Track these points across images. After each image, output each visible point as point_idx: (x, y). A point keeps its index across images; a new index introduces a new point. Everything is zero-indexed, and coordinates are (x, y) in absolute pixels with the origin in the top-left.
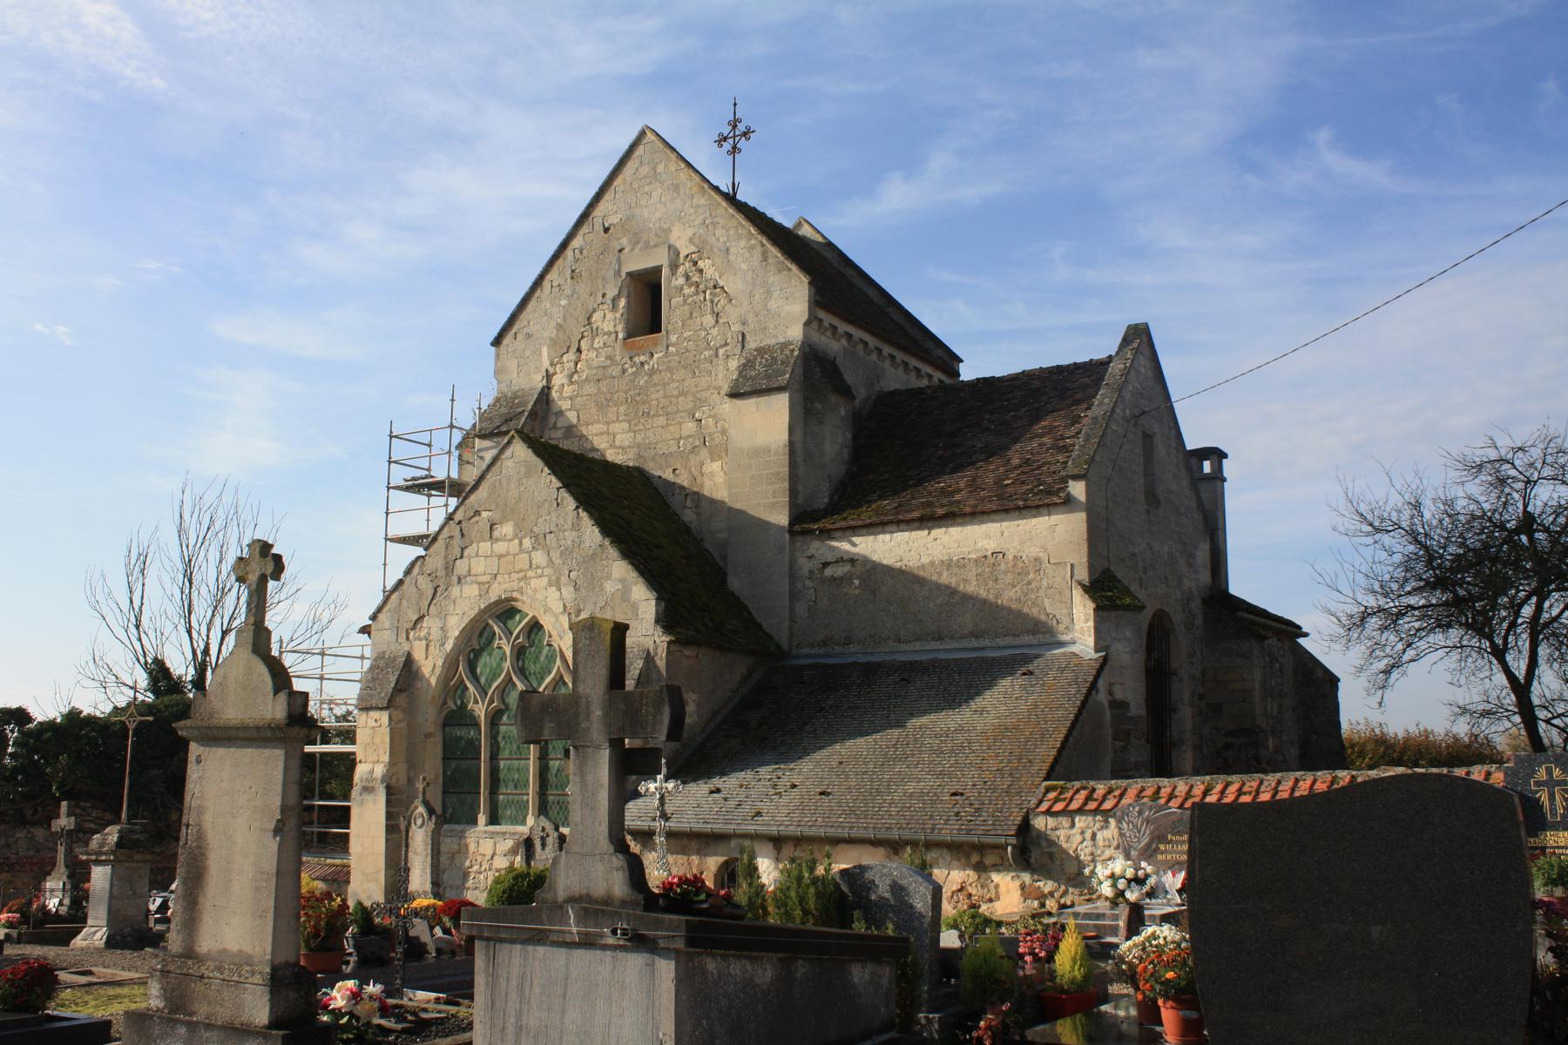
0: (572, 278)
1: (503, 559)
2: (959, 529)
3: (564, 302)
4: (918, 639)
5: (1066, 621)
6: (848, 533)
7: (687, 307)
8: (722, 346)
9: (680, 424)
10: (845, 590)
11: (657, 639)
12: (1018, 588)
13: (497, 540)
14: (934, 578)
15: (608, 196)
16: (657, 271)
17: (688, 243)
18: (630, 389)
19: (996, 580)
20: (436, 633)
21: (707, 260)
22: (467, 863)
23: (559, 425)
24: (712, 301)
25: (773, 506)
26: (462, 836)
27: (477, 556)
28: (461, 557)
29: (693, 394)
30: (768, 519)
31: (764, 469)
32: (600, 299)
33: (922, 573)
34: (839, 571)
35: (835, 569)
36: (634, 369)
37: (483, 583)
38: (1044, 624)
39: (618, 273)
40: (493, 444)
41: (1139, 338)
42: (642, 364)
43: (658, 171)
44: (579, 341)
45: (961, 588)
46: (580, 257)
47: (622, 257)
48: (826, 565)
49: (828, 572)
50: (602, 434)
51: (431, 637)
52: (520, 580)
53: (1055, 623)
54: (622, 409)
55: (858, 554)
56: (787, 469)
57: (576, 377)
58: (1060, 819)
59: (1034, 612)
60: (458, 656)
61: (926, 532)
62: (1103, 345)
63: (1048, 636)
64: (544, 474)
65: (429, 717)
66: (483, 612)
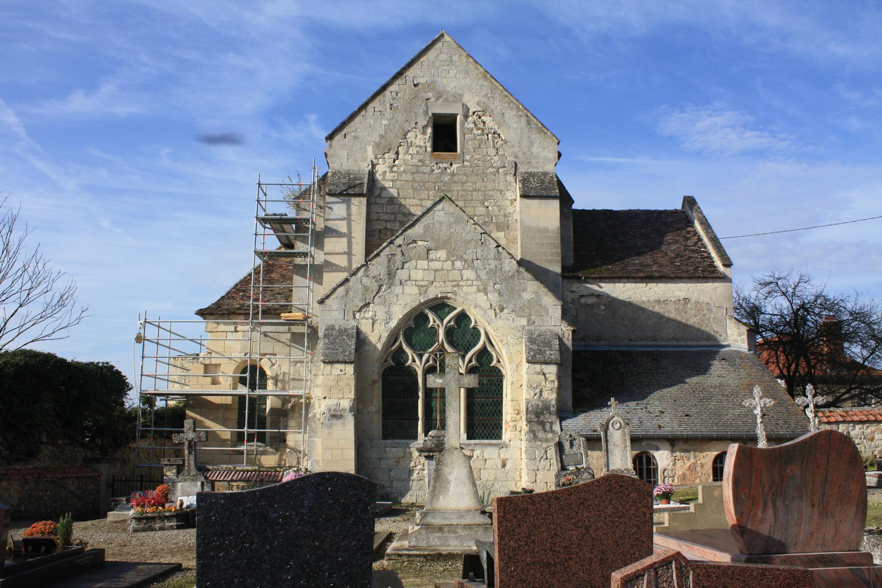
0: (391, 109)
1: (438, 273)
2: (664, 284)
3: (384, 122)
4: (641, 340)
5: (724, 335)
6: (597, 281)
7: (476, 141)
8: (501, 168)
9: (475, 207)
10: (596, 311)
11: (563, 328)
12: (698, 317)
13: (433, 260)
14: (650, 308)
15: (417, 66)
16: (454, 117)
17: (476, 105)
18: (437, 182)
19: (686, 312)
20: (381, 315)
21: (488, 117)
22: (412, 464)
23: (383, 195)
24: (494, 141)
25: (551, 261)
26: (407, 446)
27: (416, 268)
28: (402, 268)
29: (483, 191)
30: (548, 268)
31: (545, 240)
32: (414, 125)
33: (643, 306)
34: (590, 301)
35: (587, 299)
36: (440, 171)
37: (422, 286)
38: (713, 336)
39: (426, 112)
40: (341, 201)
41: (690, 202)
42: (446, 169)
43: (454, 59)
44: (398, 147)
45: (666, 315)
46: (396, 97)
47: (429, 103)
48: (582, 296)
49: (583, 300)
50: (416, 205)
51: (376, 318)
52: (454, 286)
53: (718, 336)
54: (431, 193)
55: (603, 292)
56: (559, 242)
57: (395, 169)
58: (832, 425)
59: (708, 330)
60: (399, 331)
61: (645, 284)
62: (676, 204)
63: (715, 342)
64: (469, 224)
65: (375, 371)
66: (421, 304)
